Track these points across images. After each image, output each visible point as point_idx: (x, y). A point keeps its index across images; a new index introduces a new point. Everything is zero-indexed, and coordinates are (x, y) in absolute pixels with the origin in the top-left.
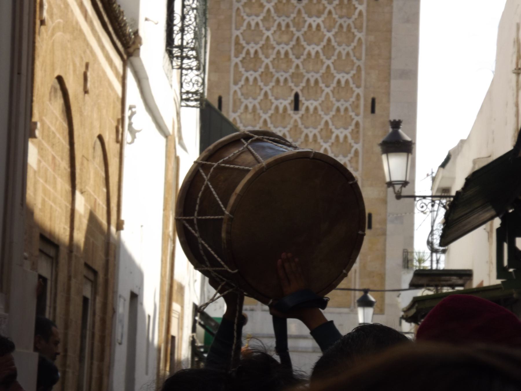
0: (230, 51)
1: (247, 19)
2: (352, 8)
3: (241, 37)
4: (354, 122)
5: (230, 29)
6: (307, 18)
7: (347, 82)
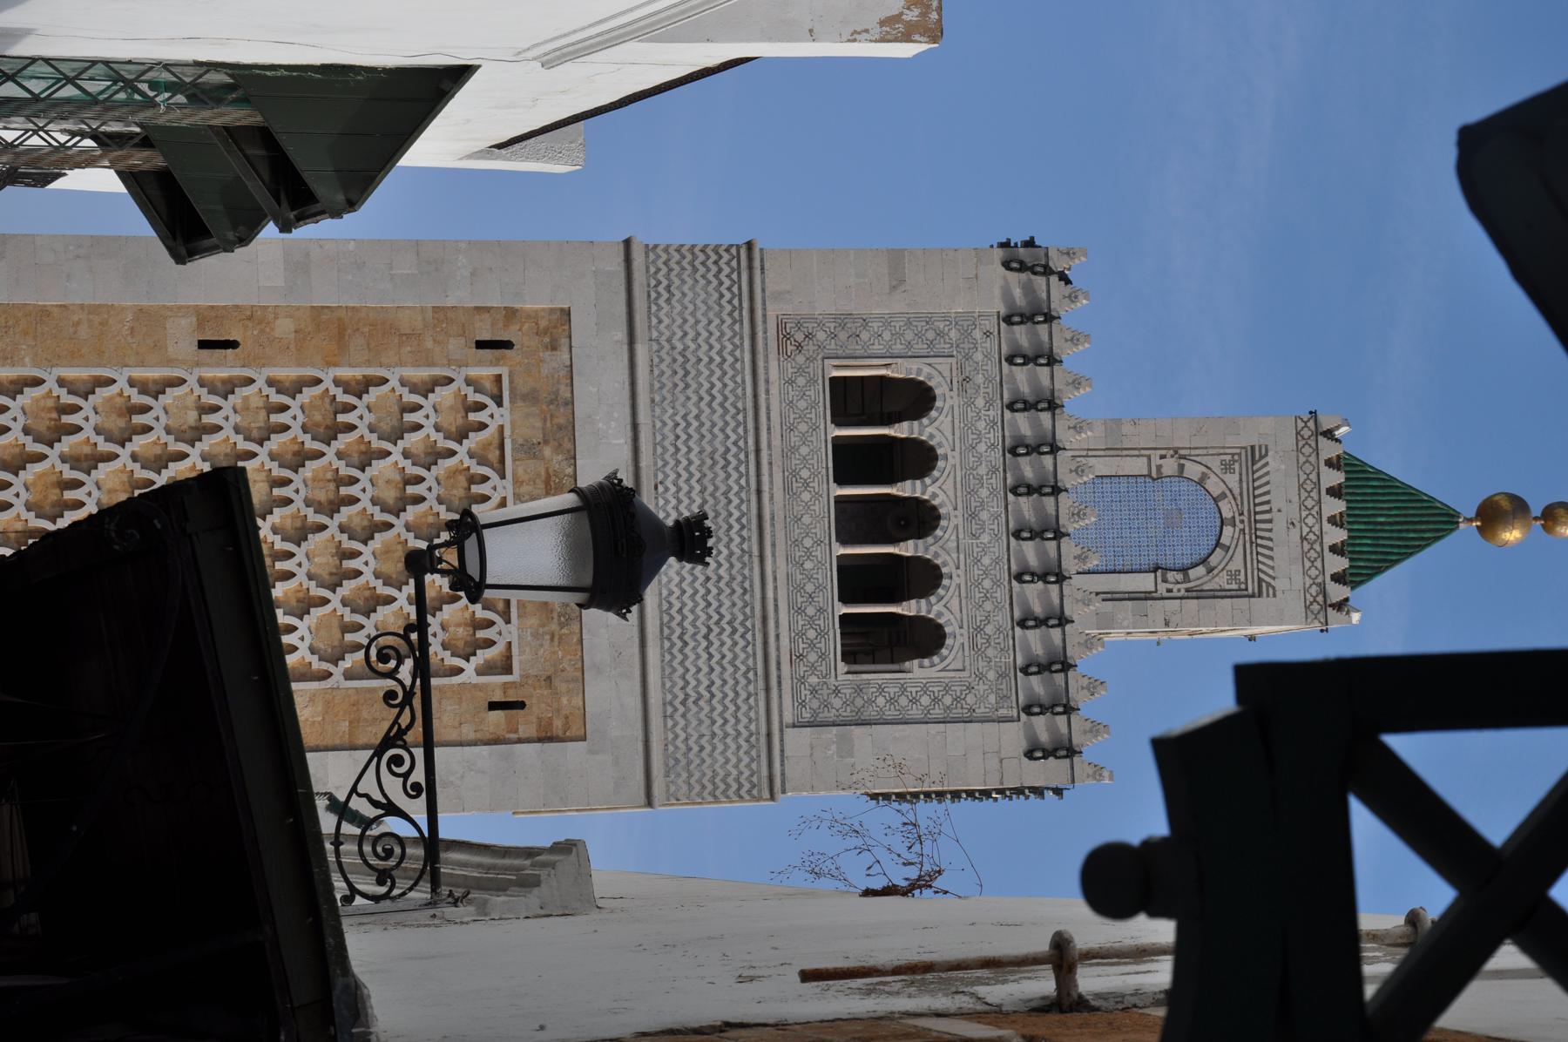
0: (351, 366)
5: (401, 364)
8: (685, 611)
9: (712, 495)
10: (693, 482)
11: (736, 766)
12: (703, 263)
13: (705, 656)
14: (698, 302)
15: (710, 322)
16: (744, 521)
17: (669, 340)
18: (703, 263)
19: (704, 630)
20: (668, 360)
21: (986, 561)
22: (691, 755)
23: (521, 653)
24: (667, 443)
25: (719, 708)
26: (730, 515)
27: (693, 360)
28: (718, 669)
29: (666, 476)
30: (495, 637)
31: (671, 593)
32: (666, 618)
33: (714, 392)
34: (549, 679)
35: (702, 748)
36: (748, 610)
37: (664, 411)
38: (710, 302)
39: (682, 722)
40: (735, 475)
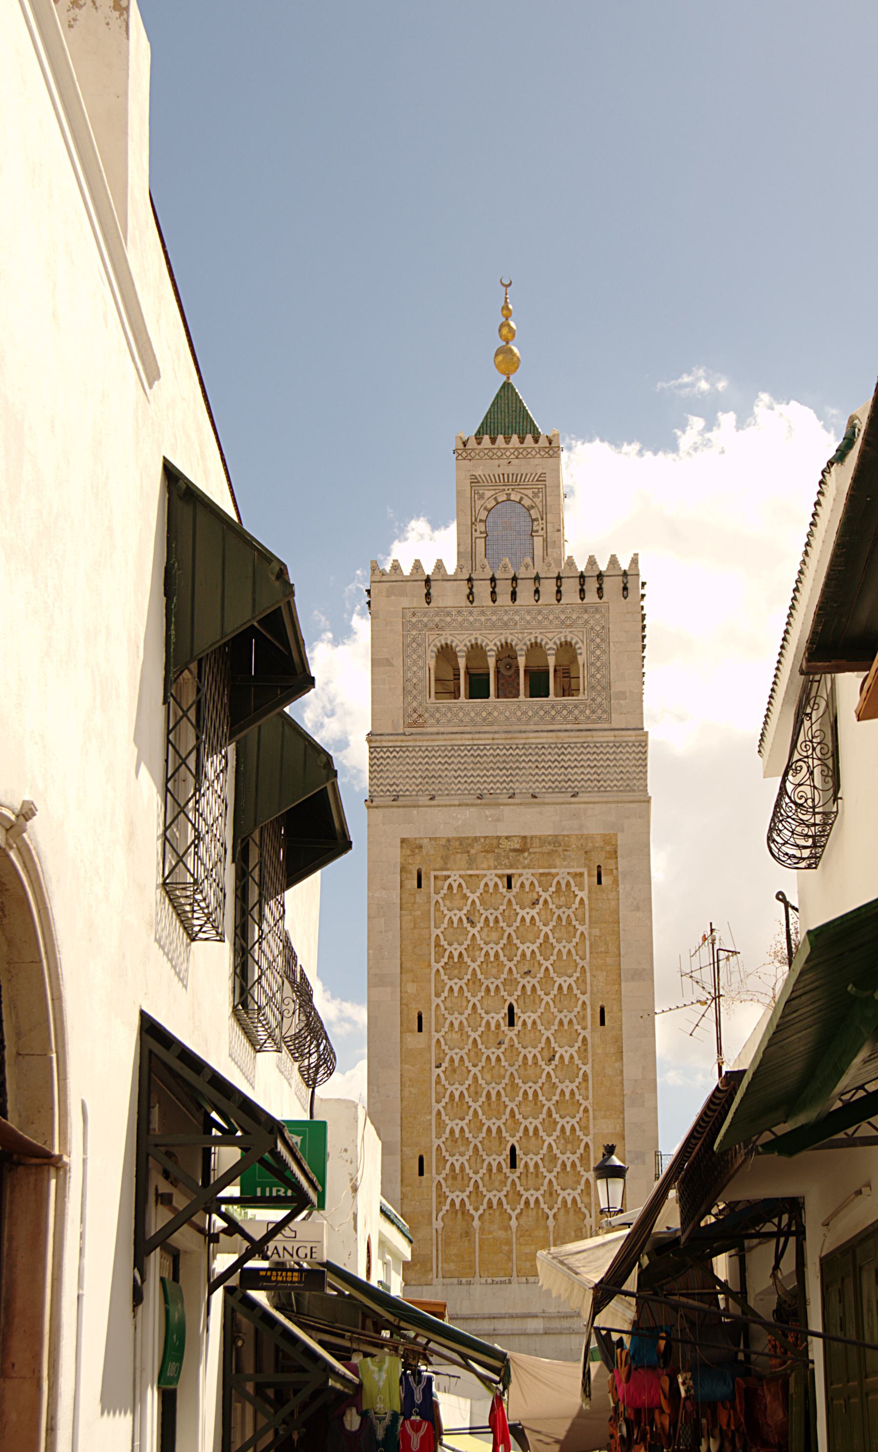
0: (430, 954)
1: (449, 914)
2: (572, 895)
3: (441, 936)
4: (581, 1037)
6: (518, 910)
7: (570, 987)
8: (553, 779)
9: (495, 764)
10: (488, 774)
11: (630, 754)
12: (378, 766)
13: (575, 769)
14: (398, 769)
15: (408, 763)
16: (508, 747)
17: (417, 786)
18: (378, 766)
19: (563, 770)
20: (427, 786)
21: (528, 618)
22: (625, 778)
23: (573, 867)
24: (469, 788)
25: (602, 762)
26: (505, 754)
27: (427, 773)
28: (582, 763)
29: (485, 788)
30: (565, 881)
31: (544, 787)
32: (557, 790)
33: (443, 762)
34: (586, 852)
35: (621, 772)
36: (553, 746)
37: (453, 789)
38: (398, 763)
39: (609, 782)
40: (485, 752)
